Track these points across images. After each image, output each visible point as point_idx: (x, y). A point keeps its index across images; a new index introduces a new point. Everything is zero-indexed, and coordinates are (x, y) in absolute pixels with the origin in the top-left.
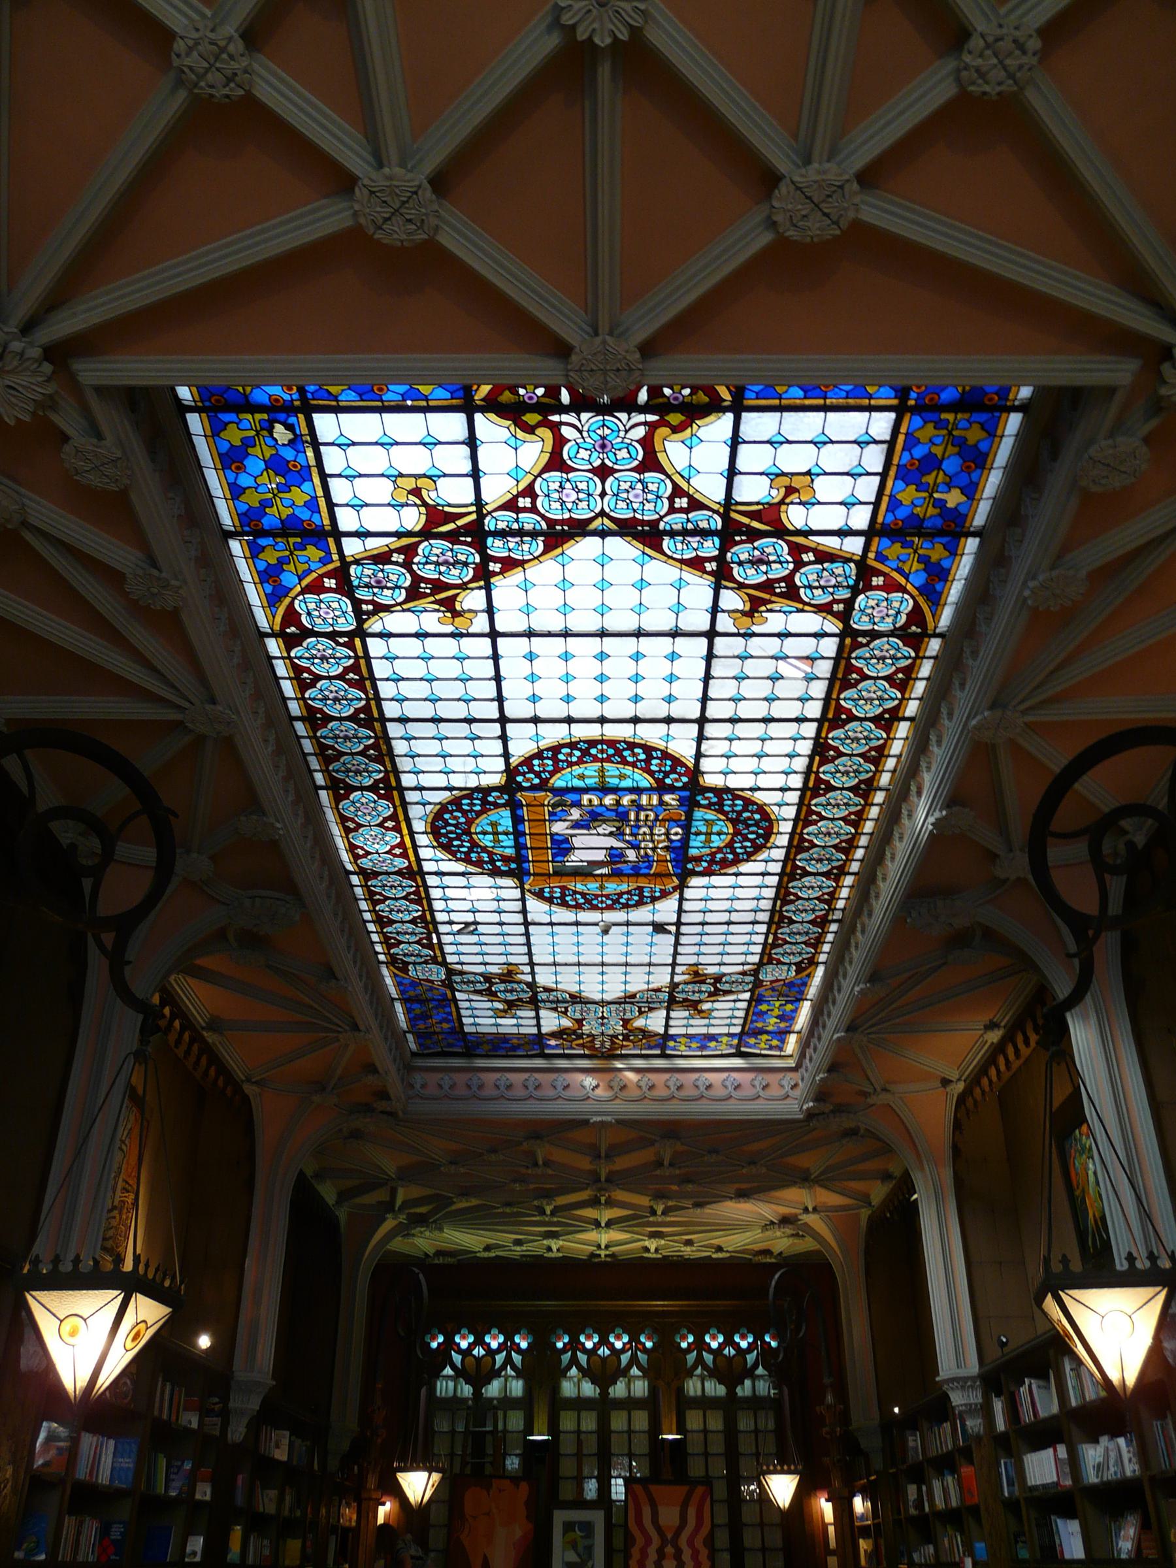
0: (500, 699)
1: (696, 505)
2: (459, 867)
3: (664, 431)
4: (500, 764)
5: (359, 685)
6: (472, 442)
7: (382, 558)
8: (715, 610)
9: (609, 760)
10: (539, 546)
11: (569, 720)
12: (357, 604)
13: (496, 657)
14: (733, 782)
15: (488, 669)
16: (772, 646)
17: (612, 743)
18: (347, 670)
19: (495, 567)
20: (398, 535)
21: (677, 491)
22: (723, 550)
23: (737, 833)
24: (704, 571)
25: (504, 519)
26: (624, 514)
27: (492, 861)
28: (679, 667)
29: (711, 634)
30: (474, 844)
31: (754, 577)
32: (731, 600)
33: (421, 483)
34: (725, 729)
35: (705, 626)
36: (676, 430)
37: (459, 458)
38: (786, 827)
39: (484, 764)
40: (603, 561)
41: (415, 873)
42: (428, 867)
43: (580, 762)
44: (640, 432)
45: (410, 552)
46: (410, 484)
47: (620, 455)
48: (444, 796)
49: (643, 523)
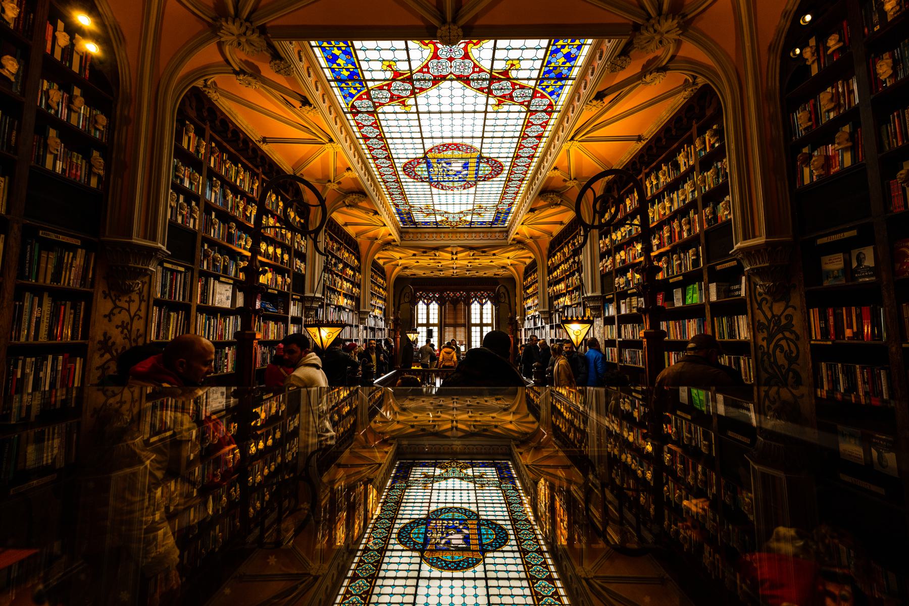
0: (421, 132)
1: (481, 70)
2: (412, 180)
3: (470, 45)
4: (422, 151)
5: (377, 128)
6: (407, 49)
7: (381, 88)
8: (487, 104)
9: (455, 149)
10: (430, 84)
11: (442, 138)
12: (374, 103)
13: (419, 119)
14: (492, 156)
15: (417, 123)
16: (505, 115)
17: (455, 144)
18: (373, 123)
19: (416, 91)
20: (384, 80)
21: (475, 66)
22: (490, 85)
23: (493, 170)
24: (483, 92)
25: (420, 75)
26: (458, 73)
27: (421, 178)
28: (476, 122)
29: (486, 112)
30: (416, 174)
31: (499, 93)
32: (492, 101)
33: (392, 63)
34: (490, 140)
35: (484, 110)
36: (475, 44)
37: (403, 55)
38: (508, 168)
39: (417, 151)
40: (451, 88)
41: (398, 181)
42: (402, 180)
43: (446, 150)
44: (463, 45)
45: (389, 85)
46: (387, 63)
47: (457, 53)
48: (406, 161)
49: (464, 76)
